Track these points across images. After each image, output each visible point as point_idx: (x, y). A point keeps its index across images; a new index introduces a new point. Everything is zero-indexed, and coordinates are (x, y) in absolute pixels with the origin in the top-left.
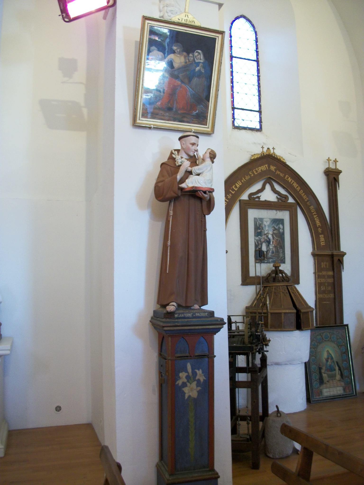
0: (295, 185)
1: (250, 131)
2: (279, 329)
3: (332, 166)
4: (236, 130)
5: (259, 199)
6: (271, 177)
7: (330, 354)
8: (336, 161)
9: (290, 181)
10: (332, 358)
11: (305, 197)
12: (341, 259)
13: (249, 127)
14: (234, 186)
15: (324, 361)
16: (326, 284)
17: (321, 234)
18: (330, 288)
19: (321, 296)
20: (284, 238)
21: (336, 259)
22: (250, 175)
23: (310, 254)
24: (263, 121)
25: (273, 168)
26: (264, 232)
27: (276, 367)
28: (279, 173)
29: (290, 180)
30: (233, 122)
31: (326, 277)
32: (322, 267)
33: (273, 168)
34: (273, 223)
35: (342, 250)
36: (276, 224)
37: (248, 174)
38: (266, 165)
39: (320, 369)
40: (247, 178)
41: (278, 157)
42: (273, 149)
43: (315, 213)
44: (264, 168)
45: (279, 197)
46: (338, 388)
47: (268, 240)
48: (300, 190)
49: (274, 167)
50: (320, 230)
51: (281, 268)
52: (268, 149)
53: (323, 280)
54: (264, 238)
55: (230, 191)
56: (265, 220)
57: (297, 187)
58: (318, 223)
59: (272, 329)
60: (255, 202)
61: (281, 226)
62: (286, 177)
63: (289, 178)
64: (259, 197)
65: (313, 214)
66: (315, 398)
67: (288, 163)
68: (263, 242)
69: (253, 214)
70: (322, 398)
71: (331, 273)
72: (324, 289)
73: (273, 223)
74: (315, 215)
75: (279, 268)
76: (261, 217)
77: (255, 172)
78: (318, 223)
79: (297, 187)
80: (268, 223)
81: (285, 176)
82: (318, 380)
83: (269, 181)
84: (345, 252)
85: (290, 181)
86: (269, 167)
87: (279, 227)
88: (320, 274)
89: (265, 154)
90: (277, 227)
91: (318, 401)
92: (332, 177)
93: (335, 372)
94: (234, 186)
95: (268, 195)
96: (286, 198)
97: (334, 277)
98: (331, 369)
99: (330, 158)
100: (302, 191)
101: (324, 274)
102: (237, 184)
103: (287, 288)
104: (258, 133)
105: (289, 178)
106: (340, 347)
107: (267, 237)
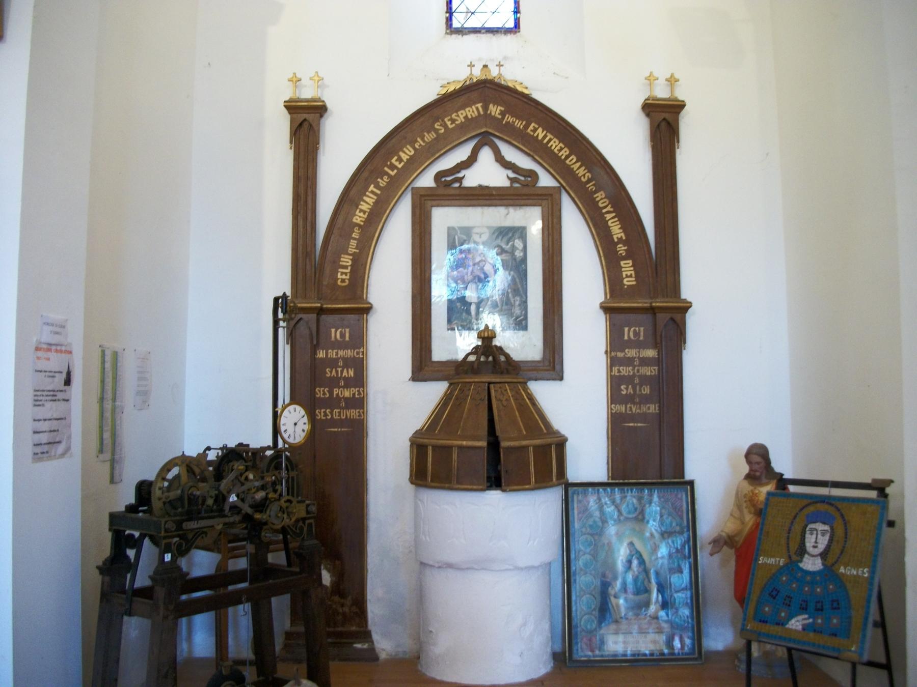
0: (555, 145)
1: (489, 35)
2: (447, 485)
3: (662, 92)
4: (454, 36)
5: (461, 183)
6: (490, 131)
7: (638, 552)
8: (672, 81)
9: (540, 137)
10: (642, 562)
11: (581, 172)
12: (677, 317)
13: (486, 26)
14: (396, 158)
15: (620, 566)
16: (637, 381)
17: (624, 258)
18: (646, 390)
19: (621, 408)
20: (526, 271)
21: (662, 318)
22: (436, 131)
23: (598, 306)
24: (522, 8)
25: (495, 110)
26: (473, 259)
27: (451, 573)
28: (511, 119)
29: (540, 133)
30: (449, 20)
31: (637, 363)
32: (626, 338)
33: (495, 110)
34: (497, 237)
35: (683, 296)
36: (505, 239)
37: (431, 129)
38: (479, 105)
39: (605, 586)
40: (429, 137)
41: (510, 85)
42: (500, 65)
43: (609, 208)
44: (471, 112)
45: (512, 175)
46: (651, 636)
47: (482, 276)
48: (567, 157)
49: (500, 108)
50: (622, 249)
51: (497, 342)
52: (485, 66)
53: (626, 371)
54: (472, 272)
55: (386, 169)
56: (475, 230)
57: (560, 150)
58: (617, 231)
59: (433, 484)
60: (451, 190)
61: (518, 244)
62: (531, 127)
63: (540, 130)
64: (460, 180)
65: (604, 211)
66: (580, 654)
67: (537, 96)
68: (472, 281)
69: (444, 218)
70: (602, 656)
71: (651, 353)
72: (630, 391)
73: (497, 237)
74: (608, 212)
75: (491, 342)
76: (466, 223)
77: (449, 123)
78: (617, 231)
79: (560, 150)
80: (485, 237)
81: (526, 127)
82: (596, 613)
83: (485, 140)
84: (689, 300)
85: (540, 137)
86: (486, 108)
87: (513, 246)
88: (620, 355)
89: (475, 80)
90: (507, 247)
91: (589, 664)
92: (664, 121)
93: (646, 595)
94: (396, 158)
95: (486, 173)
96: (533, 175)
97: (657, 362)
98: (642, 590)
99: (656, 74)
100: (573, 157)
101: (629, 355)
102: (402, 154)
103: (489, 388)
104: (510, 37)
105: (540, 130)
106: (666, 535)
107: (482, 269)
